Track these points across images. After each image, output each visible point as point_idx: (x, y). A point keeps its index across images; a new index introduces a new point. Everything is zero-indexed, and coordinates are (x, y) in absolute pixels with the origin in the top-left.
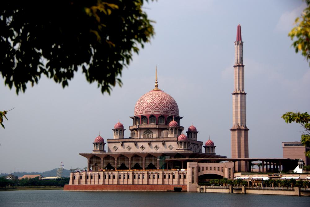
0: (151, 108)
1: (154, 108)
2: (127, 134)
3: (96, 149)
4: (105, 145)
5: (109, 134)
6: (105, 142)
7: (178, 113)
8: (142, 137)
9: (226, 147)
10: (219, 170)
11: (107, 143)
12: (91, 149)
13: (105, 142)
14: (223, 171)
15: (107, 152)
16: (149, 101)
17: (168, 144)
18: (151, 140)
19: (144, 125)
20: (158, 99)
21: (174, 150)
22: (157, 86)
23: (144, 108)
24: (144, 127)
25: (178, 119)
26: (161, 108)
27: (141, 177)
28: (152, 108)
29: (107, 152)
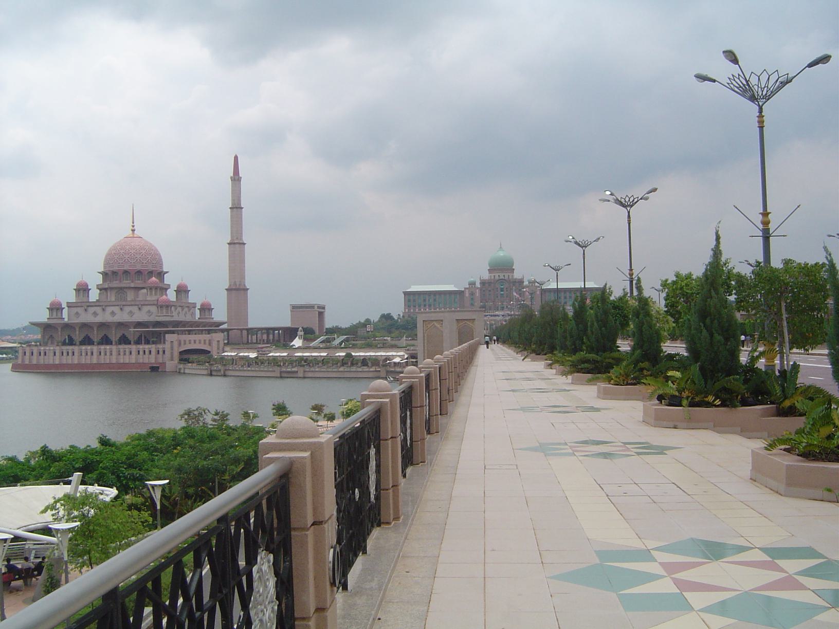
2: (94, 295)
7: (161, 267)
8: (113, 299)
9: (220, 314)
10: (205, 343)
12: (43, 316)
14: (210, 344)
15: (66, 320)
17: (146, 309)
18: (124, 303)
19: (115, 284)
21: (153, 318)
22: (133, 231)
24: (116, 286)
25: (161, 275)
27: (108, 354)
29: (66, 320)
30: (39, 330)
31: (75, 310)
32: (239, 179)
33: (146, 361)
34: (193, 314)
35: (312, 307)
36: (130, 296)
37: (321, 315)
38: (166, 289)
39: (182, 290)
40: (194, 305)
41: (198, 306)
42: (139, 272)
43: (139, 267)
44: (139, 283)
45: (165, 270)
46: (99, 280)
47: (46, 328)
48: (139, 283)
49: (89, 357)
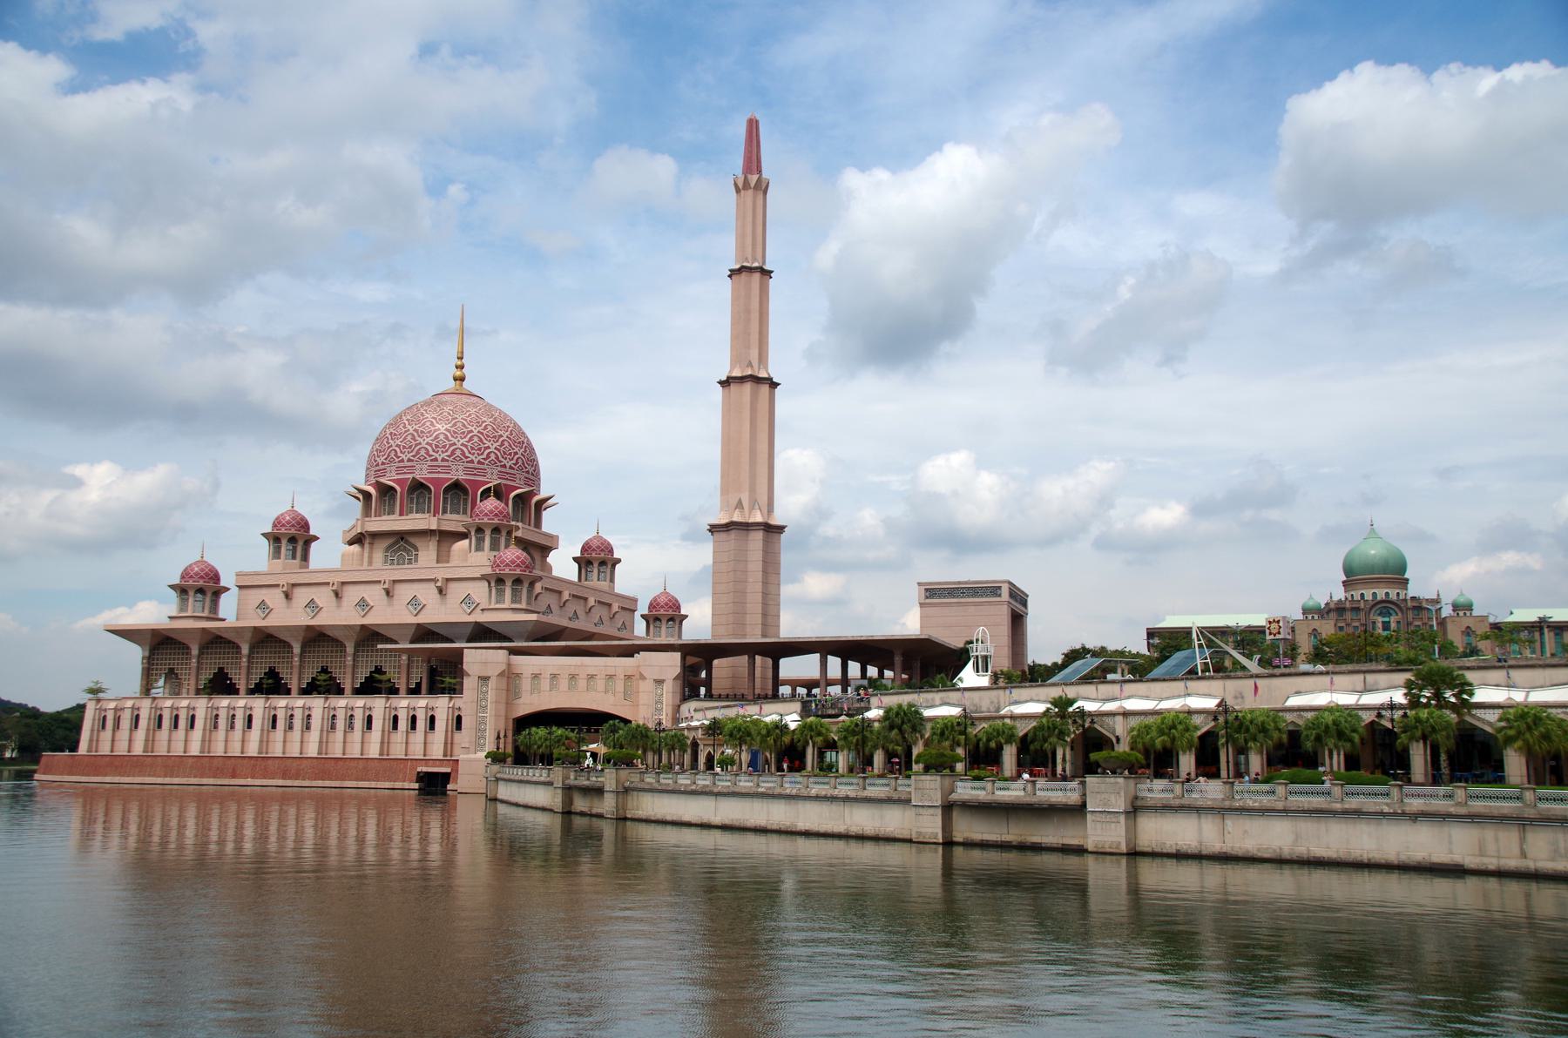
0: (453, 453)
1: (463, 453)
3: (181, 610)
4: (224, 598)
5: (242, 554)
6: (223, 583)
11: (235, 590)
12: (157, 612)
13: (223, 583)
16: (441, 427)
20: (479, 424)
23: (423, 452)
26: (493, 457)
28: (458, 453)
30: (135, 654)
31: (256, 596)
32: (762, 188)
33: (417, 751)
34: (628, 626)
35: (994, 590)
36: (427, 553)
37: (1017, 620)
38: (545, 550)
39: (597, 559)
40: (629, 606)
41: (643, 608)
42: (457, 488)
43: (458, 474)
44: (453, 522)
45: (543, 494)
46: (352, 517)
47: (161, 648)
48: (453, 522)
49: (181, 733)
